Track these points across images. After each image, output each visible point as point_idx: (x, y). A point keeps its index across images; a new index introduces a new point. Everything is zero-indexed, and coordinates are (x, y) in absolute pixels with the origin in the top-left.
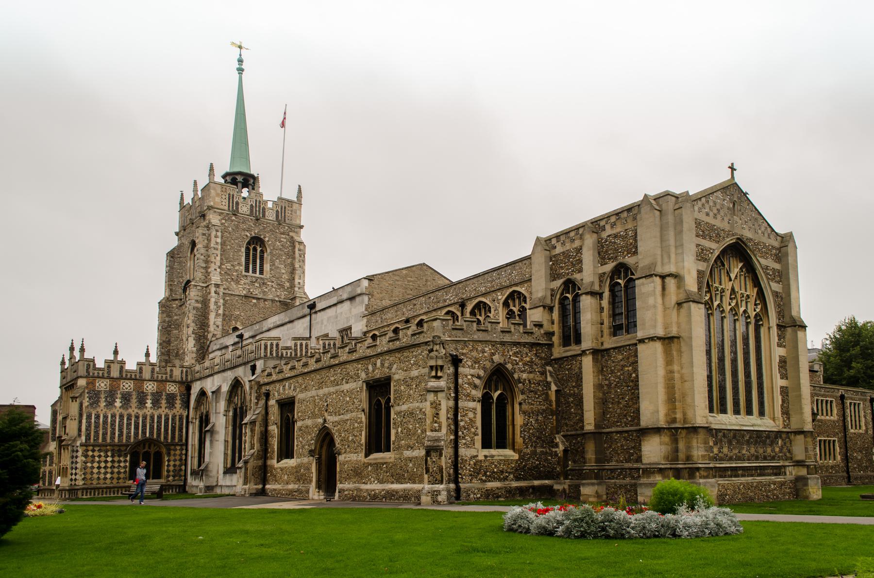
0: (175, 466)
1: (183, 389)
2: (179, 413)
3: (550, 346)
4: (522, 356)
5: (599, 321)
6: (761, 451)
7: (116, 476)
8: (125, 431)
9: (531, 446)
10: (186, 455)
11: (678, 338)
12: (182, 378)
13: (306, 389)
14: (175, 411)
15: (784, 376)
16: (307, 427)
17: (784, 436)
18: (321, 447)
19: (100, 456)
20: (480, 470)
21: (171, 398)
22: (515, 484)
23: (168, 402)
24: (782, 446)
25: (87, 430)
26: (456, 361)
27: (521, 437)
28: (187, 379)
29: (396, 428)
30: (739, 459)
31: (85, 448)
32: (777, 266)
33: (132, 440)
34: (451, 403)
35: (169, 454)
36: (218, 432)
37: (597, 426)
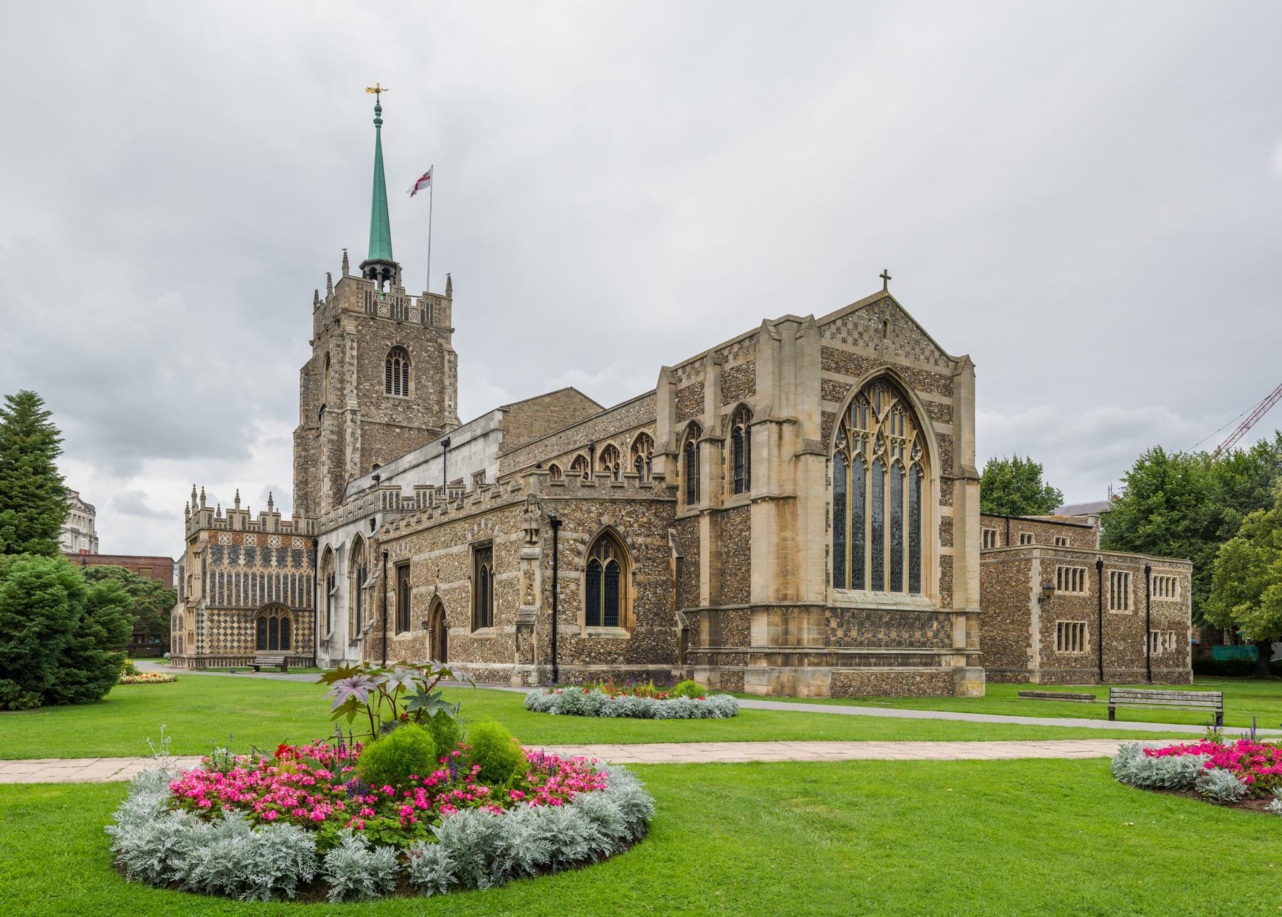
0: (303, 635)
1: (310, 544)
2: (306, 574)
3: (674, 503)
4: (637, 516)
5: (720, 475)
6: (906, 635)
7: (243, 644)
8: (250, 593)
9: (647, 624)
10: (315, 622)
11: (794, 498)
12: (308, 531)
13: (419, 551)
14: (302, 570)
15: (947, 542)
16: (421, 595)
17: (941, 617)
18: (435, 619)
19: (226, 622)
20: (581, 651)
21: (297, 555)
22: (624, 668)
23: (294, 560)
24: (938, 630)
25: (211, 591)
26: (556, 524)
27: (634, 612)
28: (313, 532)
29: (498, 600)
30: (871, 644)
31: (210, 611)
32: (946, 401)
33: (258, 604)
34: (549, 573)
35: (297, 621)
36: (342, 598)
37: (711, 602)
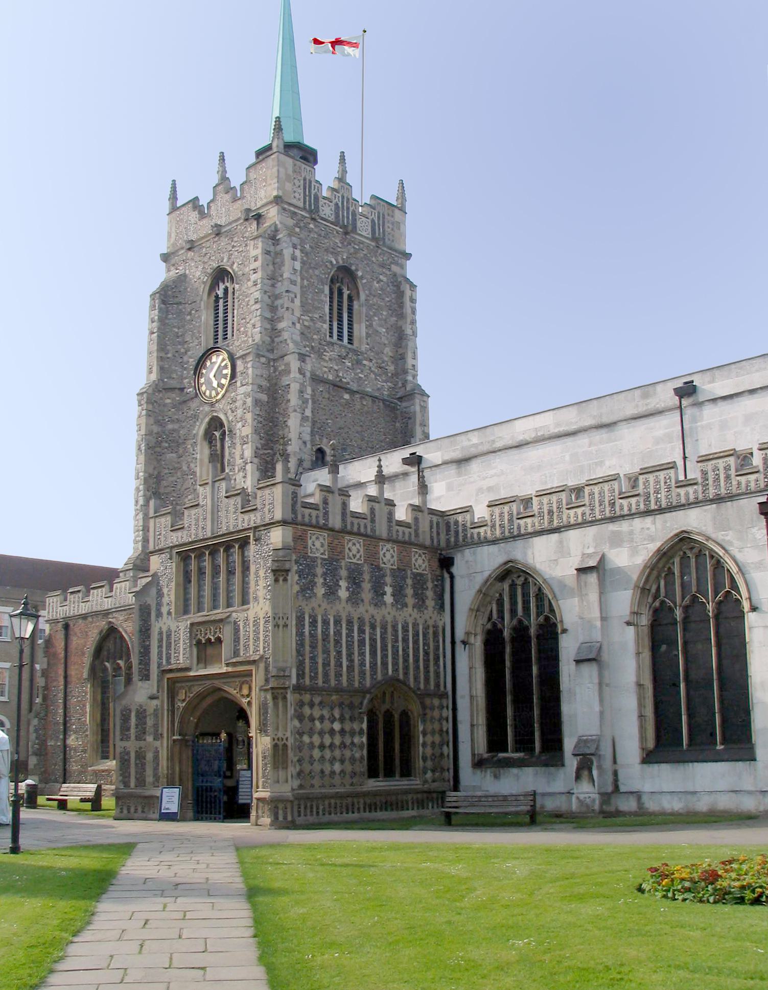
8: (356, 657)
19: (322, 719)
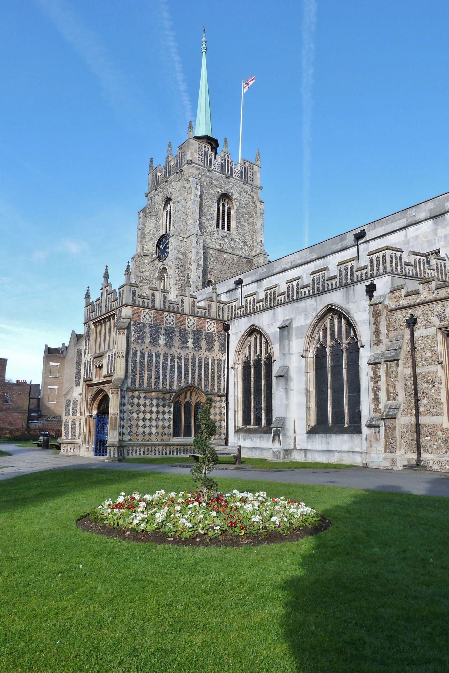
19: (145, 405)
23: (207, 343)
25: (132, 371)
